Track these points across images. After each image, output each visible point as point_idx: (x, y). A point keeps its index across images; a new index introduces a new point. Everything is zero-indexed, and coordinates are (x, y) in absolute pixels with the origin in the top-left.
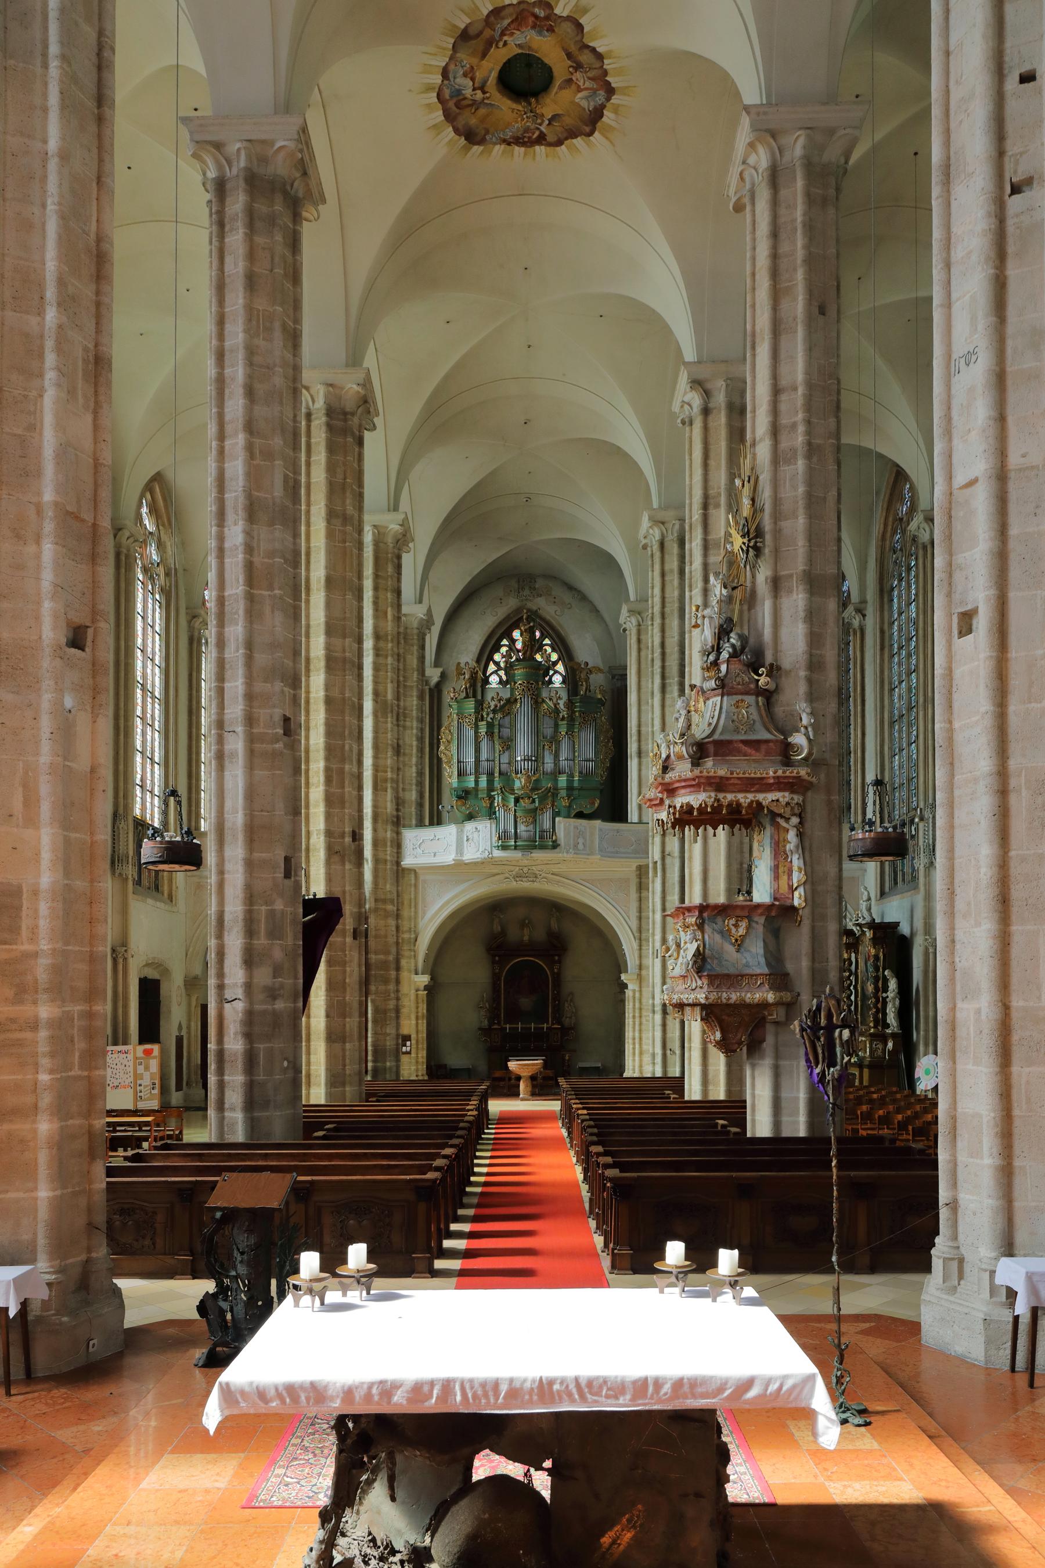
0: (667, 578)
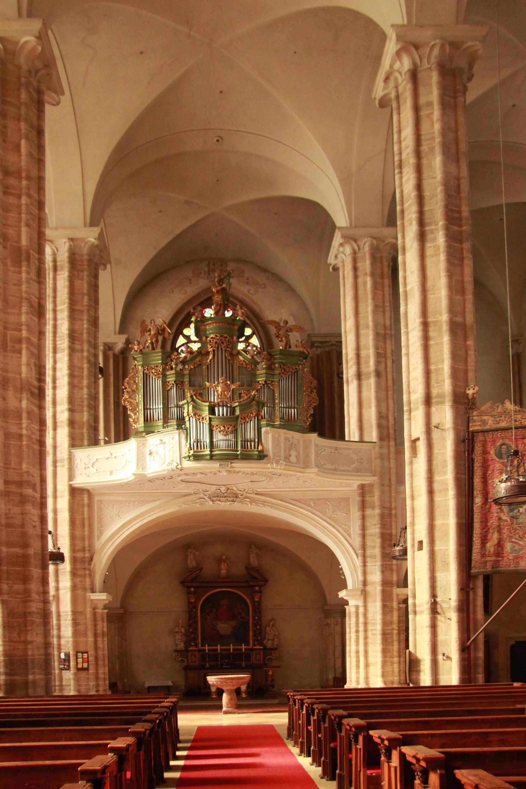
0: (423, 113)
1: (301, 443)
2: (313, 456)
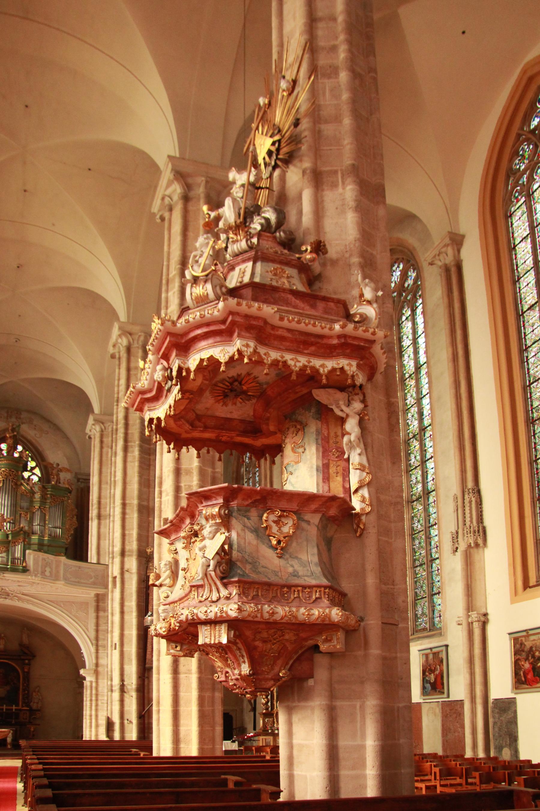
1: (54, 562)
2: (62, 572)
